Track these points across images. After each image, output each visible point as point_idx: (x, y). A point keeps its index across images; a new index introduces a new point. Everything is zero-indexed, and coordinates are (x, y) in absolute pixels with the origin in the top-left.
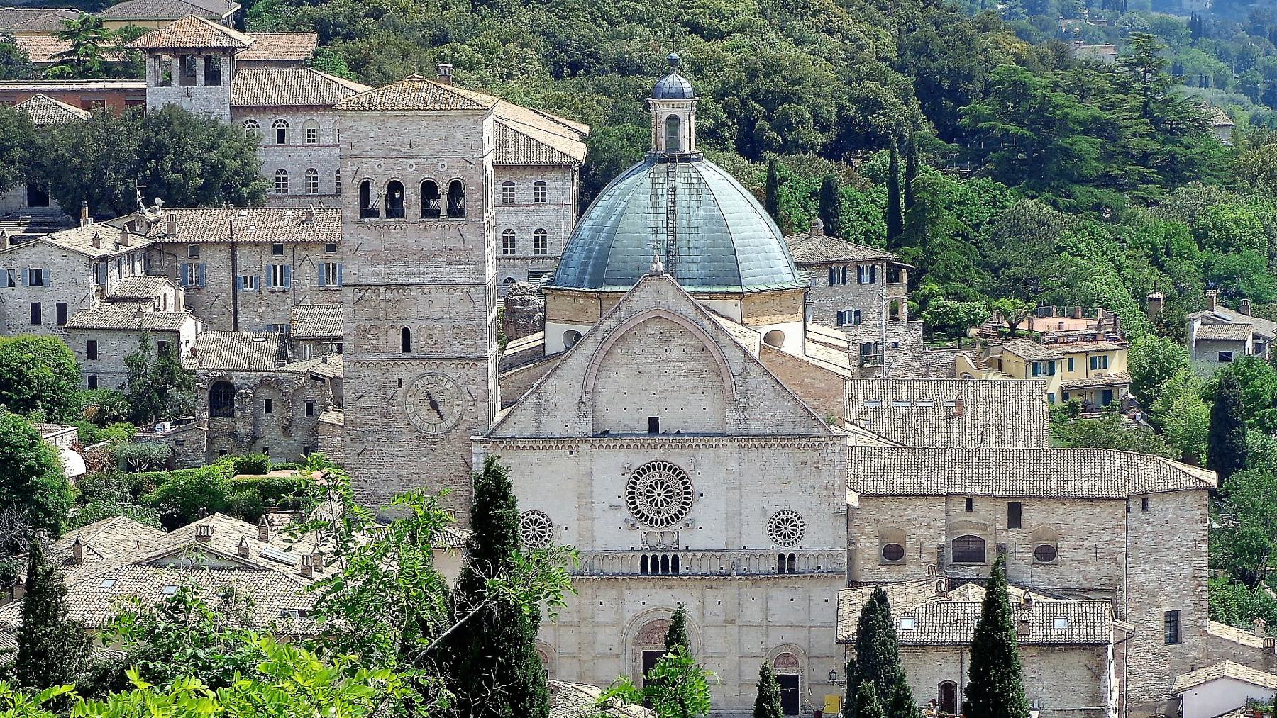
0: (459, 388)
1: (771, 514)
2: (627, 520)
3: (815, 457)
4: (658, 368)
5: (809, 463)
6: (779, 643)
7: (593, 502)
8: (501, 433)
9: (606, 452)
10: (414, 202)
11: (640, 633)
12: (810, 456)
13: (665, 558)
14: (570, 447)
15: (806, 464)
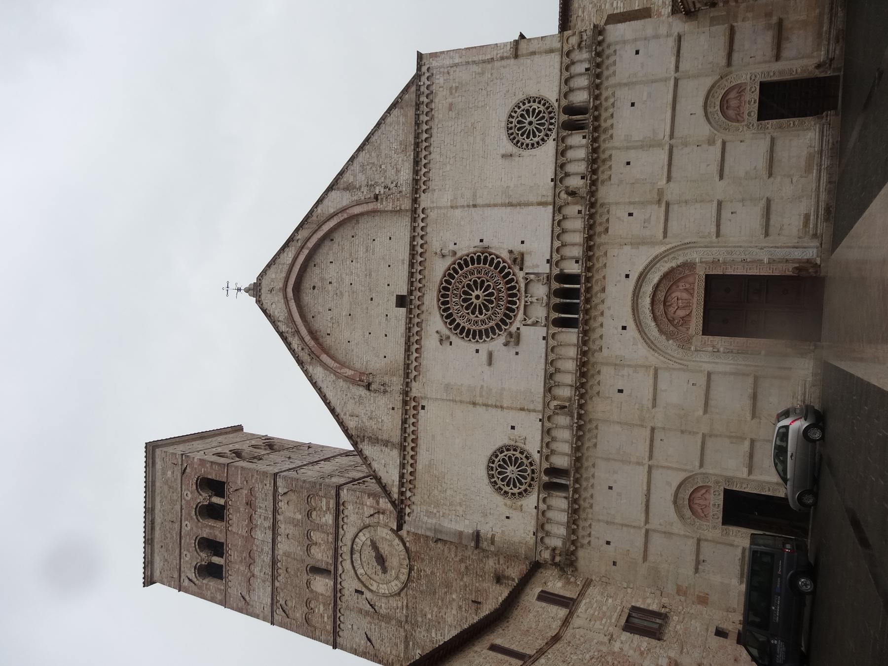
0: (366, 527)
1: (508, 147)
2: (506, 344)
3: (444, 93)
4: (347, 294)
5: (450, 100)
6: (703, 119)
7: (482, 387)
8: (395, 496)
9: (424, 363)
10: (212, 531)
11: (669, 336)
12: (440, 103)
13: (559, 293)
14: (415, 408)
15: (451, 105)
